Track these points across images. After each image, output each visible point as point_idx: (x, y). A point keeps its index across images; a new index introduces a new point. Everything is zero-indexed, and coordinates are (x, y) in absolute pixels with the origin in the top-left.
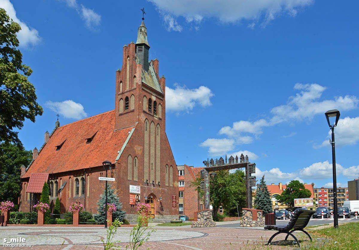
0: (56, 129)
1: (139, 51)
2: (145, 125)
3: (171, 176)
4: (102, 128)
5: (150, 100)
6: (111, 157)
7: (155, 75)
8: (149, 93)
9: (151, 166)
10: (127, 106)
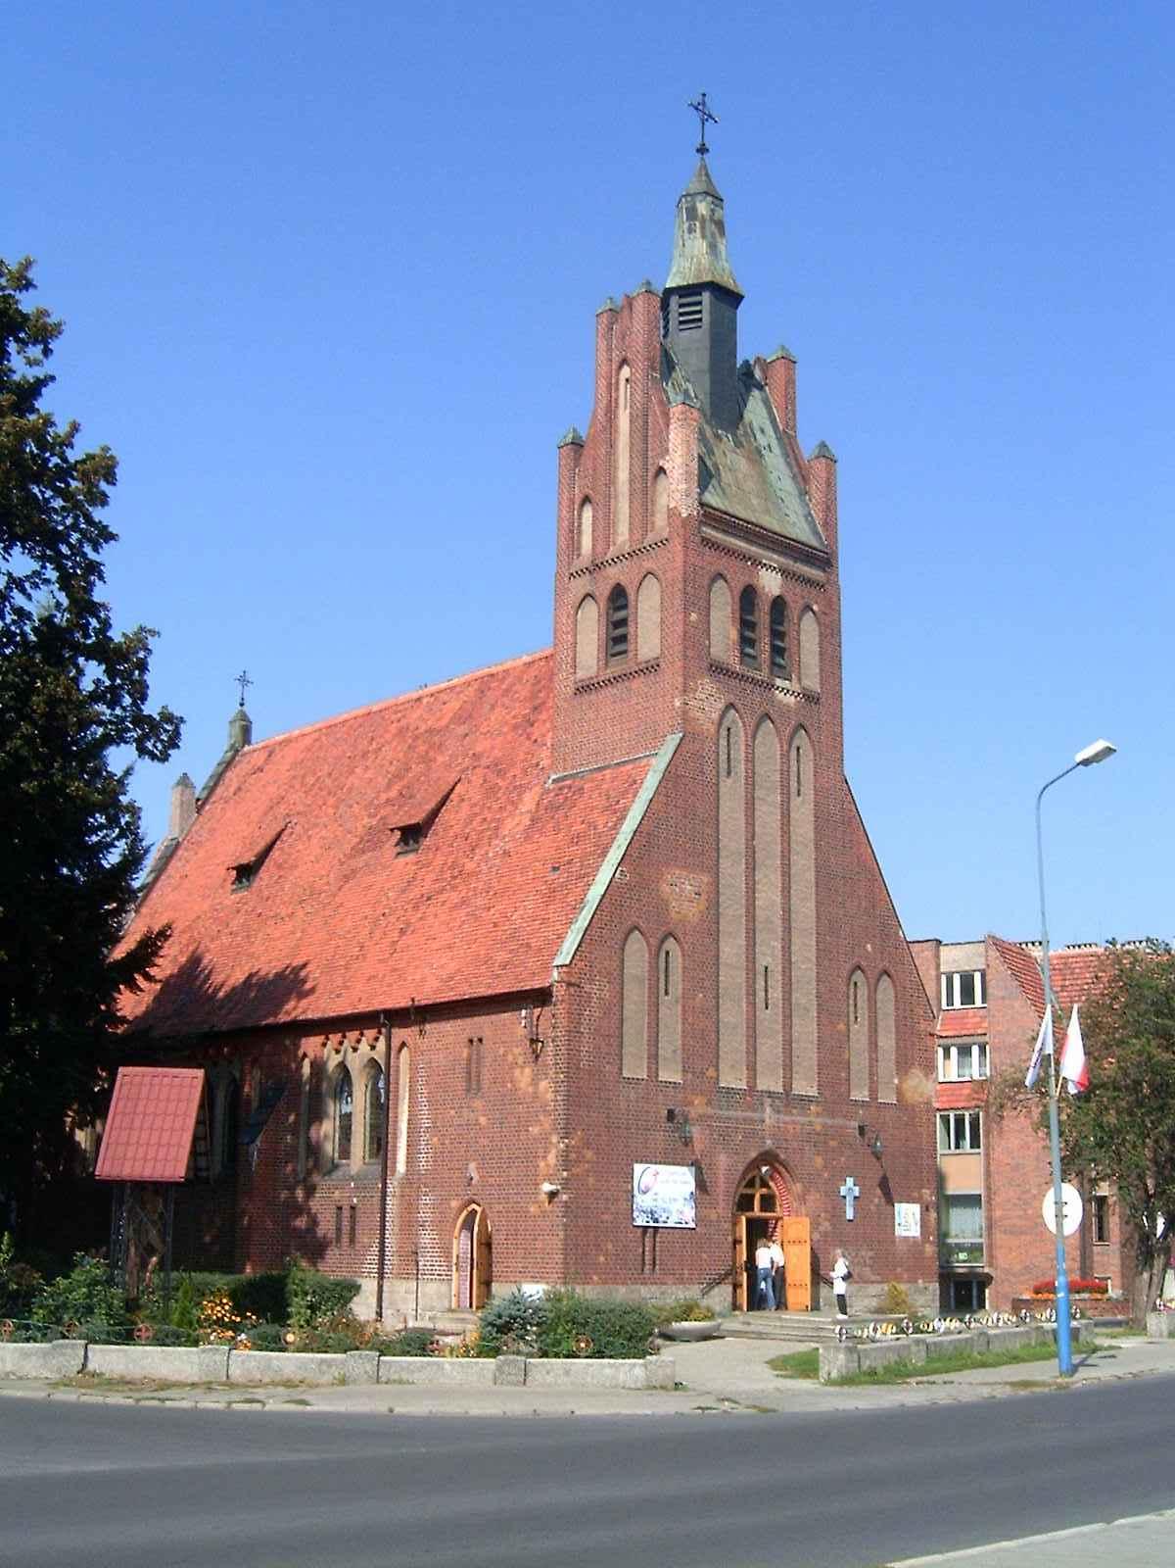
0: (233, 757)
1: (681, 323)
2: (723, 742)
3: (887, 1042)
4: (484, 762)
5: (748, 597)
6: (528, 945)
7: (774, 443)
8: (745, 557)
9: (760, 983)
10: (618, 637)
